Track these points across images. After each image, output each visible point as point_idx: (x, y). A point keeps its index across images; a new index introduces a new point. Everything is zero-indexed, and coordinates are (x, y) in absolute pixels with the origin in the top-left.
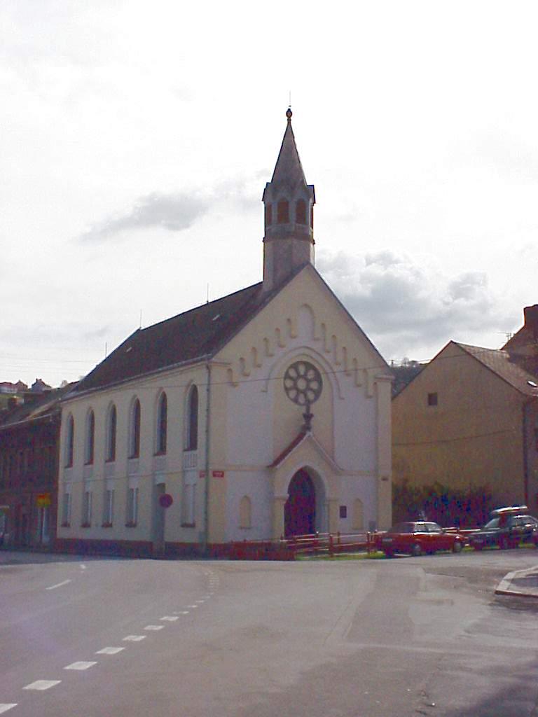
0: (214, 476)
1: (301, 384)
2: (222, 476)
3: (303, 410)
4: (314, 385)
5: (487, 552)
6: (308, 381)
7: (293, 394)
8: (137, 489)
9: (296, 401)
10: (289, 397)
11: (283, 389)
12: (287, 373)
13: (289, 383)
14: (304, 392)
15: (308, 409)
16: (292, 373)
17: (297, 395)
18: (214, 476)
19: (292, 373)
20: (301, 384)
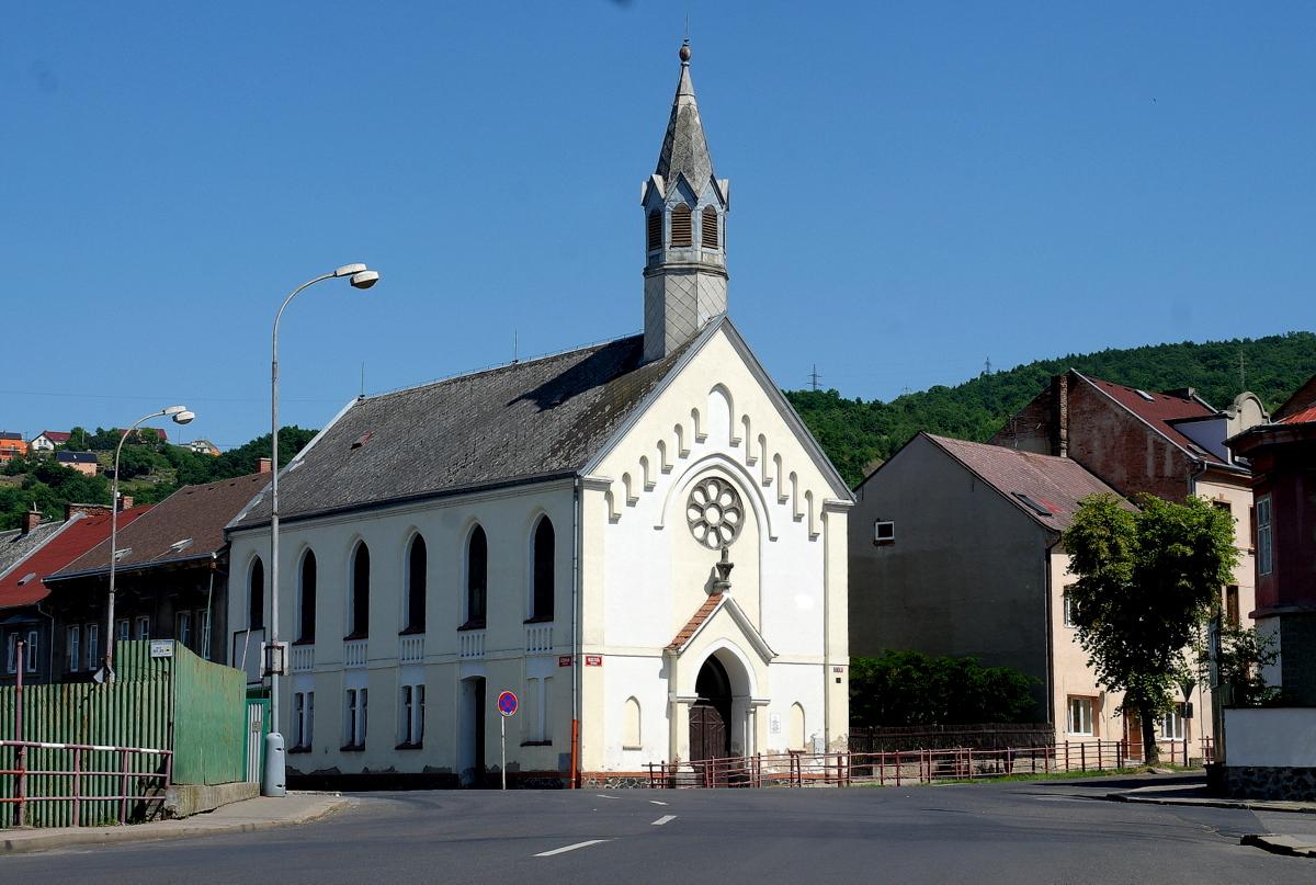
0: (588, 663)
1: (713, 516)
2: (600, 664)
3: (717, 557)
4: (731, 517)
5: (681, 361)
6: (721, 511)
7: (700, 531)
8: (311, 694)
9: (704, 542)
10: (712, 548)
11: (686, 523)
12: (691, 497)
13: (695, 515)
14: (715, 529)
15: (724, 555)
16: (699, 498)
17: (706, 534)
18: (588, 663)
19: (699, 498)
20: (713, 516)
